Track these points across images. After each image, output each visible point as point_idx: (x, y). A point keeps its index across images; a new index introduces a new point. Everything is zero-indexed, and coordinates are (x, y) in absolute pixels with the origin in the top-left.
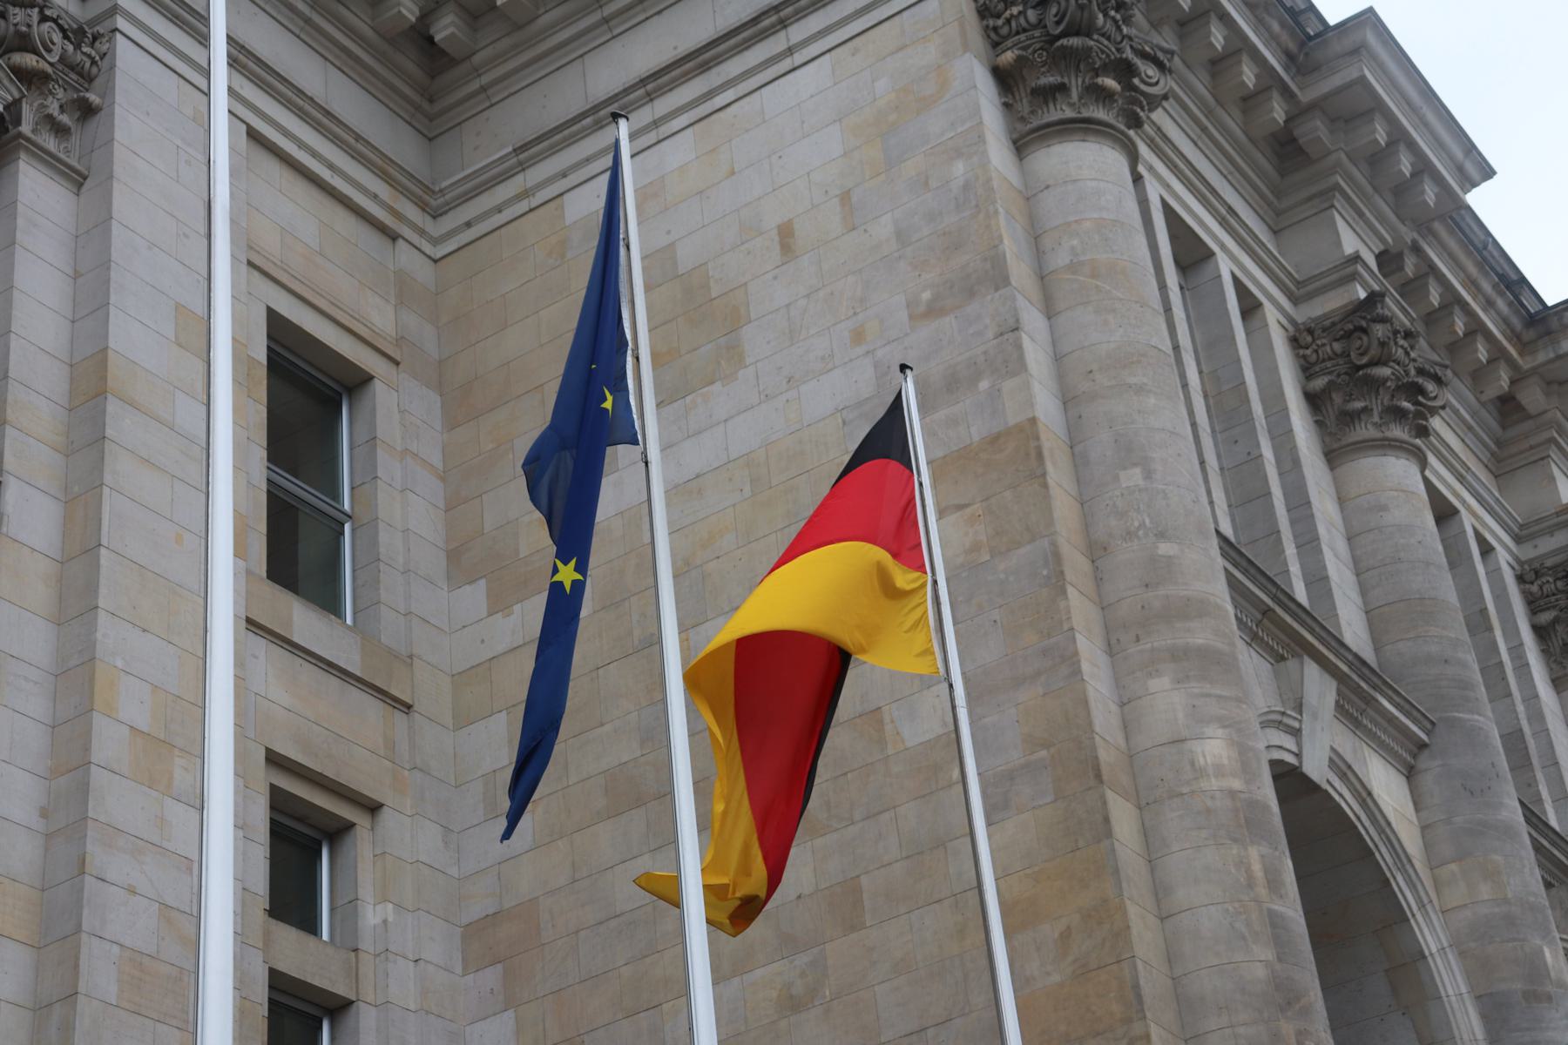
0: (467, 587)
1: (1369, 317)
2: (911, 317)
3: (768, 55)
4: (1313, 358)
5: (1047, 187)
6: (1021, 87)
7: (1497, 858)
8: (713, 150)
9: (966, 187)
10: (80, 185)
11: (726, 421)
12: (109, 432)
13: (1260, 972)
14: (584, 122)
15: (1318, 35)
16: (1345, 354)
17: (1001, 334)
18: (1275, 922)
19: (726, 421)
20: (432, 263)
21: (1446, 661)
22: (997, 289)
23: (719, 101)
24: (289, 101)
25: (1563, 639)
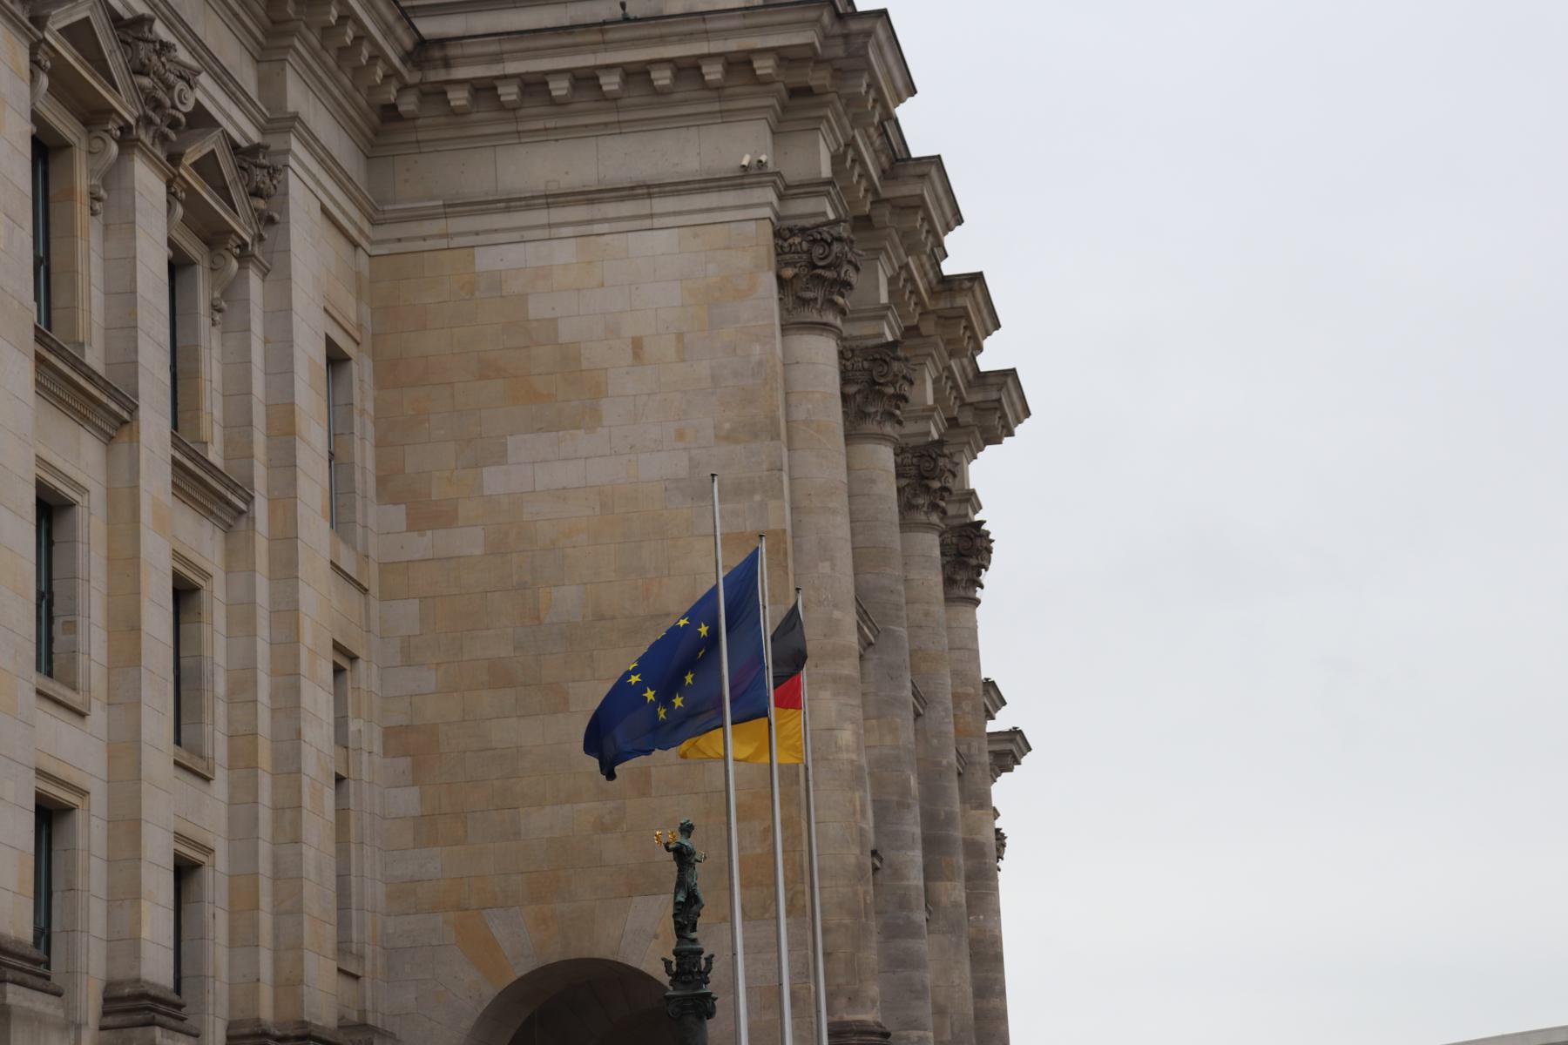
0: (391, 506)
1: (892, 355)
2: (716, 436)
3: (636, 213)
4: (850, 368)
5: (797, 363)
6: (790, 288)
7: (898, 720)
8: (590, 263)
9: (760, 364)
10: (265, 275)
11: (586, 458)
12: (298, 462)
13: (853, 860)
14: (499, 205)
15: (903, 160)
16: (870, 371)
17: (772, 470)
18: (862, 832)
19: (586, 458)
20: (367, 257)
21: (892, 591)
22: (772, 439)
23: (597, 228)
24: (336, 176)
25: (908, 498)
